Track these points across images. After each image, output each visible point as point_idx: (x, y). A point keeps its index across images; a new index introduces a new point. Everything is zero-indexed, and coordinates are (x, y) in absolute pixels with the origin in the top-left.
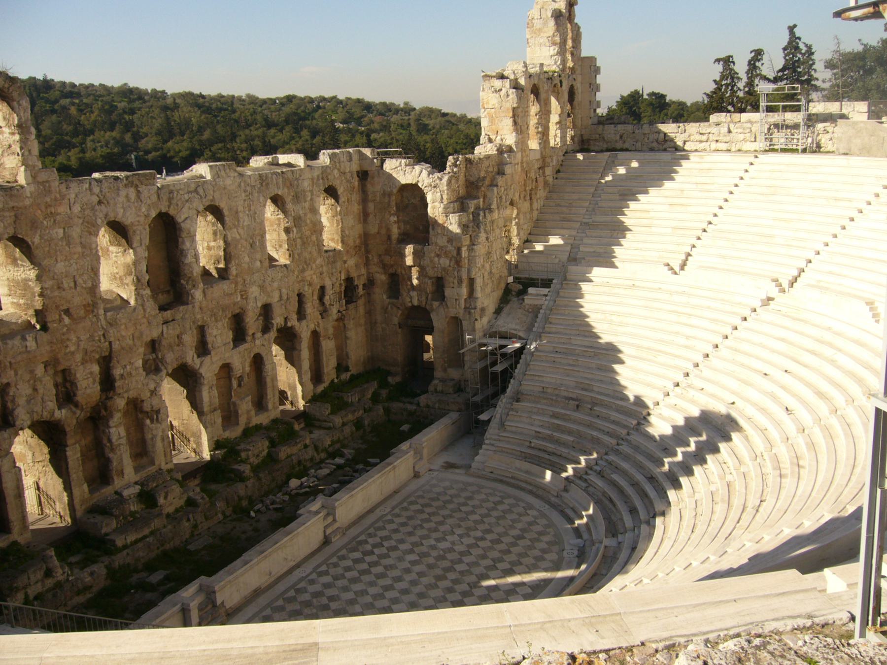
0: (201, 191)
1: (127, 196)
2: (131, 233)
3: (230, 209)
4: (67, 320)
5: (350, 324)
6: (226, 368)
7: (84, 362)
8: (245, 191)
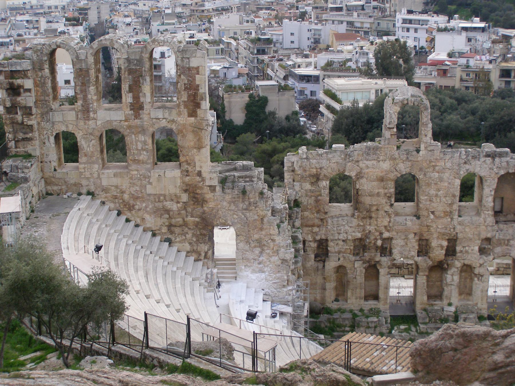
1: (485, 161)
2: (484, 181)
4: (432, 216)
7: (438, 238)
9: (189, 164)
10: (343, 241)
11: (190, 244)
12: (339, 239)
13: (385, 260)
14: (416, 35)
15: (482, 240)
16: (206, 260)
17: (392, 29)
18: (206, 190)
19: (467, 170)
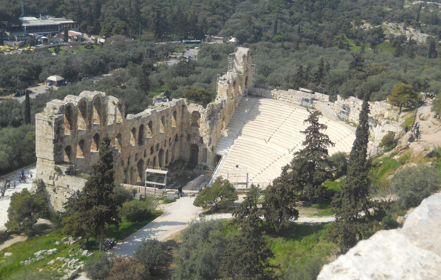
5: (176, 147)
6: (149, 159)
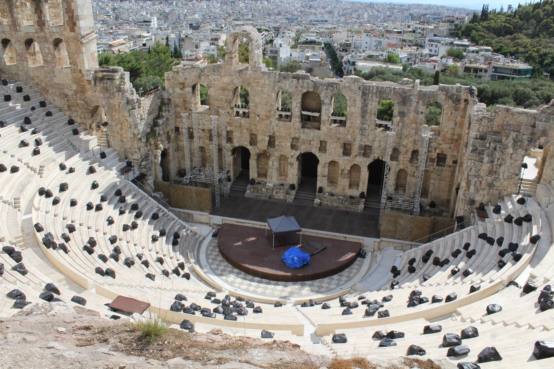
0: (335, 86)
3: (351, 97)
4: (258, 118)
8: (363, 92)
9: (74, 65)
10: (203, 130)
11: (81, 118)
12: (199, 129)
13: (228, 145)
14: (437, 49)
15: (293, 139)
16: (90, 130)
17: (423, 44)
18: (86, 83)
19: (280, 87)
